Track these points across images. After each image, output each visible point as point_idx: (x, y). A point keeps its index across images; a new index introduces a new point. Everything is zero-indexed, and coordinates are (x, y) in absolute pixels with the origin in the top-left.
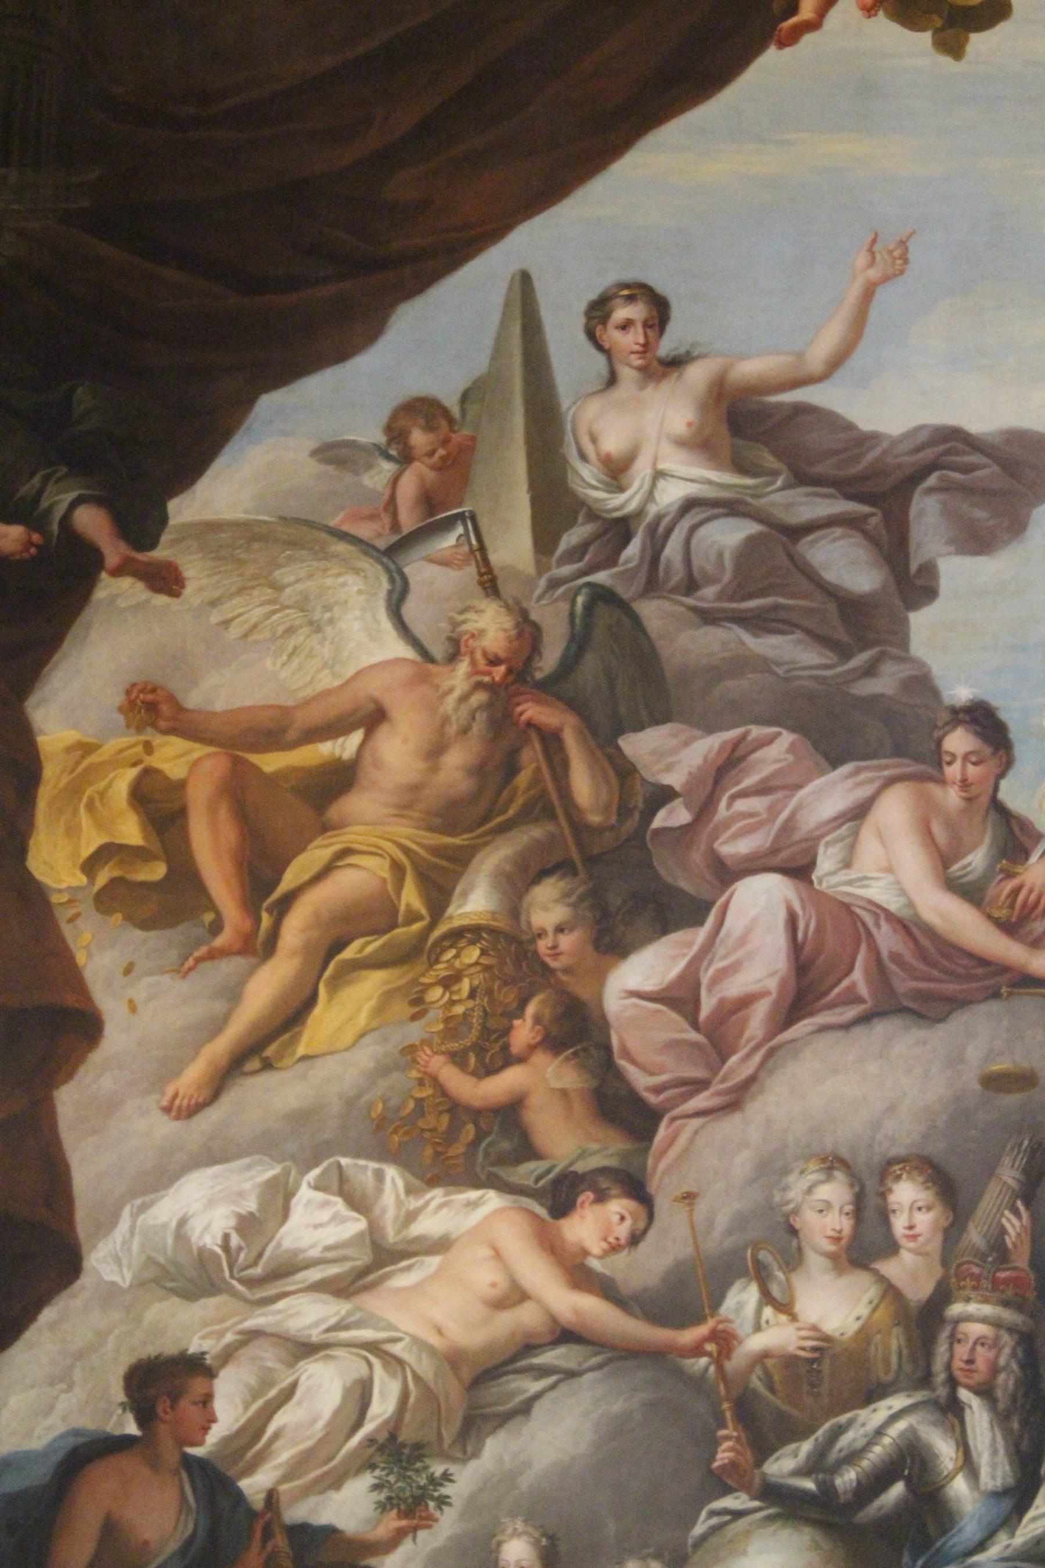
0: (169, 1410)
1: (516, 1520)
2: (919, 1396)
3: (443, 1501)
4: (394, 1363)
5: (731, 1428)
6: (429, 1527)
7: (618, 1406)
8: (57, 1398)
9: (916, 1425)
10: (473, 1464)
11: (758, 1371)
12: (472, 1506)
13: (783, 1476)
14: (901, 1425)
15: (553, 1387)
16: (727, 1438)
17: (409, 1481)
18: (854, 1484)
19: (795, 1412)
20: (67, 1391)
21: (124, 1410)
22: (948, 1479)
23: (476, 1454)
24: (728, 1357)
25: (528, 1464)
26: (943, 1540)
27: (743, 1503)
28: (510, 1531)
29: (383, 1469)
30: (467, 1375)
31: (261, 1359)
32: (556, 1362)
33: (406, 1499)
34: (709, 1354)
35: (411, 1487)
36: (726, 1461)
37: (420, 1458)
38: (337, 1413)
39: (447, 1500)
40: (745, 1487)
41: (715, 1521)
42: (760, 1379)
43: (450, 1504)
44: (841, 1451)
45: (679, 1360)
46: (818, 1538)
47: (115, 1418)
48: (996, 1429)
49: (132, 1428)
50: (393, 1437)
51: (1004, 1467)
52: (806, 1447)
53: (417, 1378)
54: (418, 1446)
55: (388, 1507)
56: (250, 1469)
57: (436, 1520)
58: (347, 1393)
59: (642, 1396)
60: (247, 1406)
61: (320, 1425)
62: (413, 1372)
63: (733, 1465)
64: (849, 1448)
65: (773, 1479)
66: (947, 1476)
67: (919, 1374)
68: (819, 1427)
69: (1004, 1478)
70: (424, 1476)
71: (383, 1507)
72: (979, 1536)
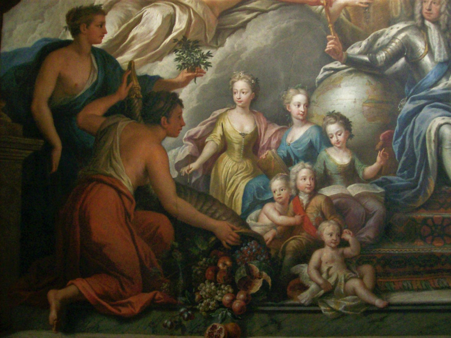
0: (86, 29)
1: (240, 72)
2: (410, 23)
3: (207, 65)
4: (185, 8)
5: (333, 35)
6: (202, 76)
7: (284, 25)
8: (37, 25)
10: (221, 49)
11: (343, 11)
12: (221, 67)
13: (356, 55)
14: (403, 35)
15: (255, 17)
16: (331, 39)
17: (192, 56)
18: (385, 58)
19: (360, 29)
21: (66, 30)
22: (422, 56)
23: (222, 45)
24: (331, 6)
25: (245, 49)
26: (421, 81)
27: (338, 66)
28: (237, 77)
29: (181, 52)
30: (217, 12)
31: (126, 7)
32: (257, 7)
33: (191, 64)
34: (322, 4)
35: (193, 59)
36: (331, 48)
37: (197, 47)
38: (160, 28)
39: (209, 64)
40: (340, 59)
41: (327, 73)
42: (344, 15)
43: (211, 66)
44: (378, 45)
46: (370, 80)
47: (62, 33)
48: (441, 37)
49: (70, 37)
50: (185, 38)
51: (444, 52)
52: (364, 43)
53: (194, 13)
54: (196, 42)
55: (183, 68)
56: (122, 53)
57: (205, 73)
58: (164, 20)
60: (120, 27)
61: (152, 33)
63: (334, 49)
65: (351, 56)
66: (422, 55)
68: (369, 36)
69: (444, 56)
70: (199, 54)
71: (180, 68)
72: (434, 80)
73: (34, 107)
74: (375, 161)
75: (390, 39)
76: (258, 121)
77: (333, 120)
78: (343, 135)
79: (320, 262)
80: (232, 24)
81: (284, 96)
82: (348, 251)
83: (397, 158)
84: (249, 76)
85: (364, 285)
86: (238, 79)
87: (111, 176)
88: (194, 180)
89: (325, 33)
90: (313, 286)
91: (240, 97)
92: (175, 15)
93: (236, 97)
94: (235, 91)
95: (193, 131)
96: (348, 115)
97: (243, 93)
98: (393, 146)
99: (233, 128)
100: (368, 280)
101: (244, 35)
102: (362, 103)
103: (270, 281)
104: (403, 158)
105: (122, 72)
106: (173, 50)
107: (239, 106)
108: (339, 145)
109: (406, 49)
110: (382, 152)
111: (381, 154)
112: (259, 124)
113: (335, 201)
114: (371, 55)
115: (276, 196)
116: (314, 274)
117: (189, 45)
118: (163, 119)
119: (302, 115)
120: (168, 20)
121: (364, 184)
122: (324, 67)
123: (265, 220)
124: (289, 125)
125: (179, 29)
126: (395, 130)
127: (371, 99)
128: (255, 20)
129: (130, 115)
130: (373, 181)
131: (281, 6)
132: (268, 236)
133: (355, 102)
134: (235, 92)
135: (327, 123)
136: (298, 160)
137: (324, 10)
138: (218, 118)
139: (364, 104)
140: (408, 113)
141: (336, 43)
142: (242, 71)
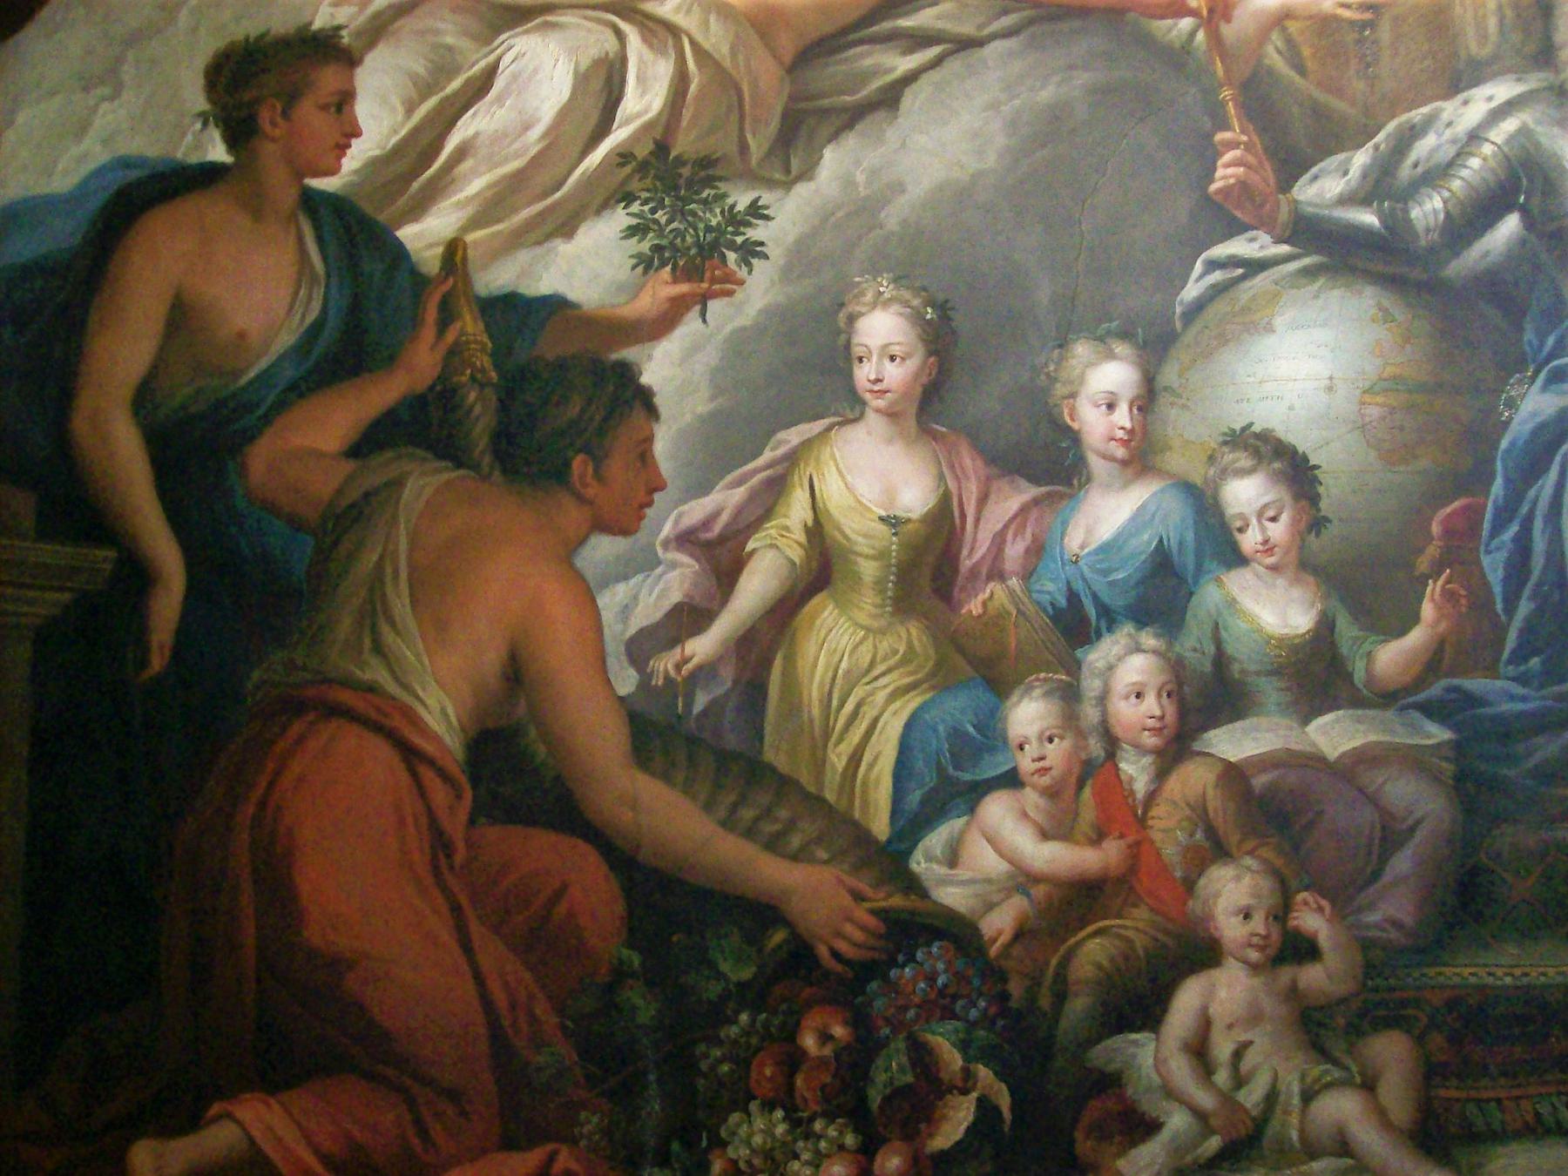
0: (279, 120)
2: (1534, 81)
3: (751, 251)
4: (660, 31)
6: (730, 293)
7: (1046, 95)
8: (95, 109)
9: (1532, 126)
10: (802, 190)
12: (802, 258)
13: (1328, 207)
14: (1510, 125)
17: (690, 218)
18: (1442, 216)
19: (1340, 105)
20: (112, 99)
21: (205, 124)
23: (807, 174)
24: (1227, 18)
25: (899, 188)
28: (869, 297)
30: (788, 46)
31: (436, 32)
32: (940, 25)
33: (689, 249)
35: (696, 229)
36: (1232, 181)
37: (709, 181)
38: (564, 114)
39: (758, 249)
40: (1266, 224)
41: (1217, 276)
42: (1279, 52)
43: (766, 257)
44: (1416, 165)
45: (1144, 21)
46: (1386, 303)
47: (189, 137)
49: (218, 153)
50: (662, 148)
52: (1360, 159)
54: (706, 163)
56: (418, 209)
57: (741, 283)
58: (581, 81)
59: (1083, 78)
60: (410, 110)
62: (693, 43)
63: (1243, 185)
64: (1428, 160)
65: (1310, 209)
67: (1531, 48)
70: (718, 211)
71: (646, 263)
73: (80, 425)
74: (1415, 619)
75: (1460, 145)
76: (952, 467)
77: (1244, 461)
78: (1285, 518)
79: (1205, 1024)
80: (844, 93)
81: (1052, 368)
82: (1312, 976)
83: (1499, 606)
84: (916, 294)
85: (1382, 1114)
86: (874, 306)
87: (371, 689)
88: (701, 701)
89: (1207, 123)
90: (1177, 1121)
91: (881, 378)
92: (624, 60)
93: (863, 374)
94: (857, 351)
95: (695, 511)
96: (1302, 439)
97: (892, 358)
98: (1486, 561)
99: (855, 496)
100: (1396, 1093)
101: (892, 135)
102: (1358, 392)
103: (1004, 1101)
104: (1524, 608)
105: (420, 282)
106: (619, 196)
107: (878, 411)
108: (1270, 560)
109: (1525, 182)
110: (1440, 583)
111: (1438, 589)
112: (958, 479)
113: (1260, 781)
114: (1386, 204)
115: (1026, 764)
116: (1181, 1070)
117: (680, 176)
118: (579, 464)
119: (1125, 443)
120: (597, 84)
121: (1371, 713)
122: (1203, 256)
123: (985, 860)
124: (1075, 482)
125: (639, 115)
126: (1492, 497)
127: (1395, 378)
128: (934, 76)
129: (450, 450)
130: (1411, 700)
131: (1031, 22)
132: (999, 923)
133: (1330, 389)
134: (861, 355)
135: (1225, 473)
136: (1110, 619)
137: (1201, 36)
138: (793, 458)
139: (1367, 398)
140: (1542, 426)
141: (1251, 159)
142: (885, 275)
